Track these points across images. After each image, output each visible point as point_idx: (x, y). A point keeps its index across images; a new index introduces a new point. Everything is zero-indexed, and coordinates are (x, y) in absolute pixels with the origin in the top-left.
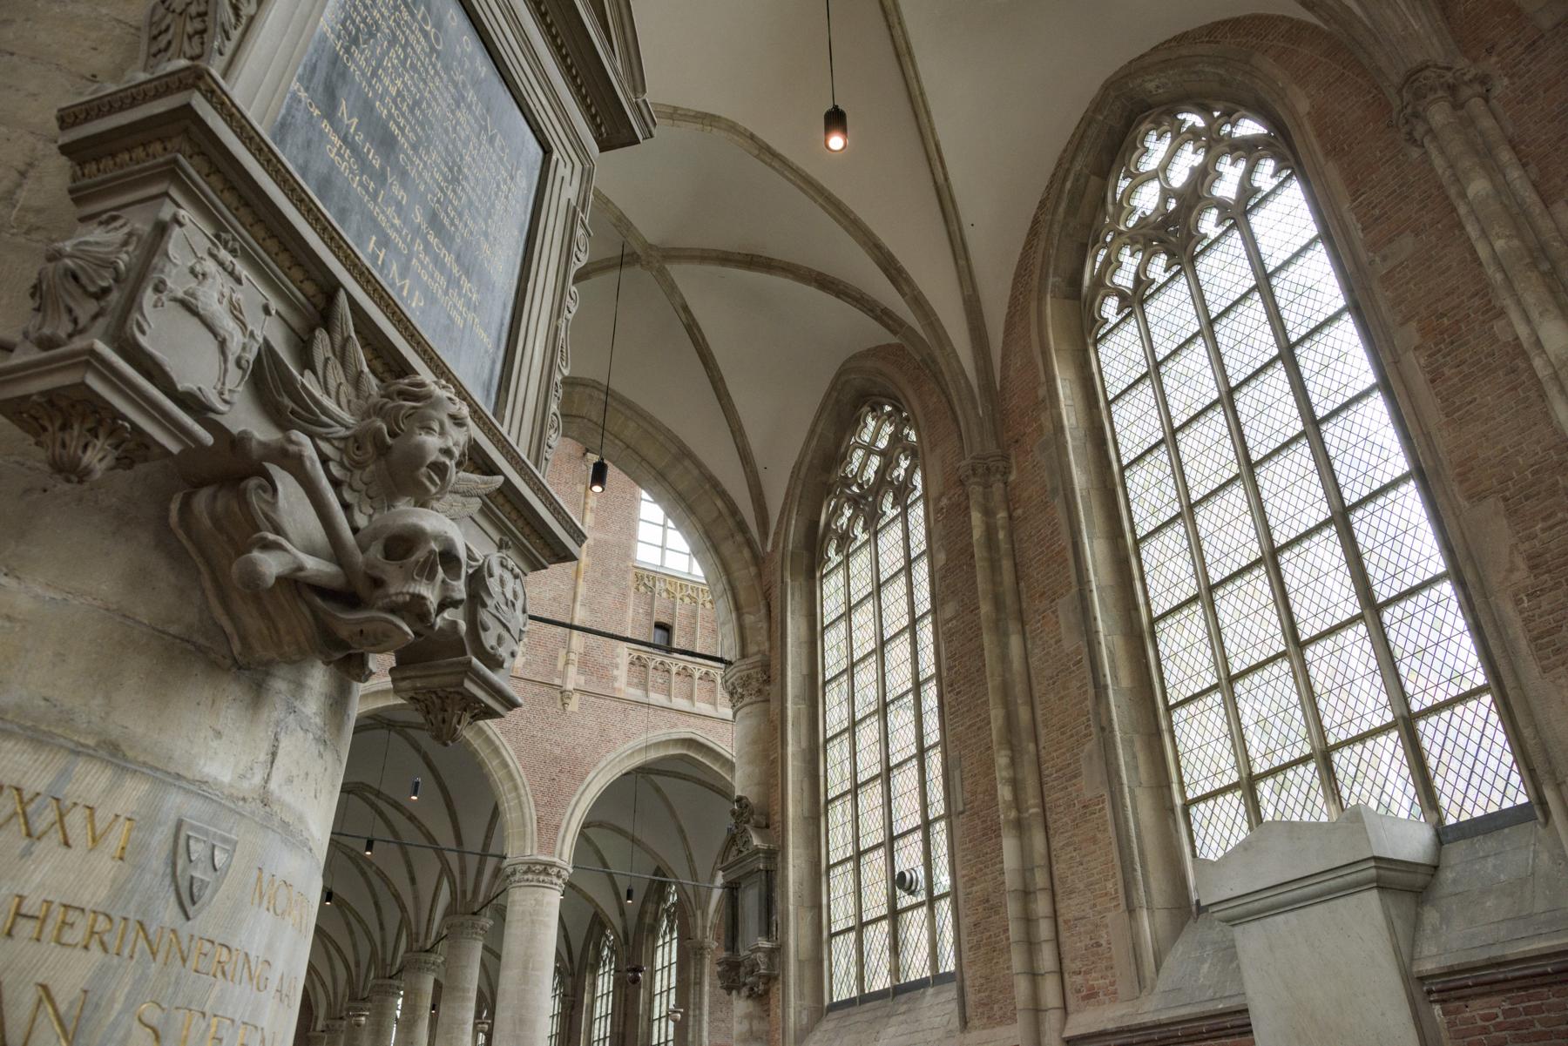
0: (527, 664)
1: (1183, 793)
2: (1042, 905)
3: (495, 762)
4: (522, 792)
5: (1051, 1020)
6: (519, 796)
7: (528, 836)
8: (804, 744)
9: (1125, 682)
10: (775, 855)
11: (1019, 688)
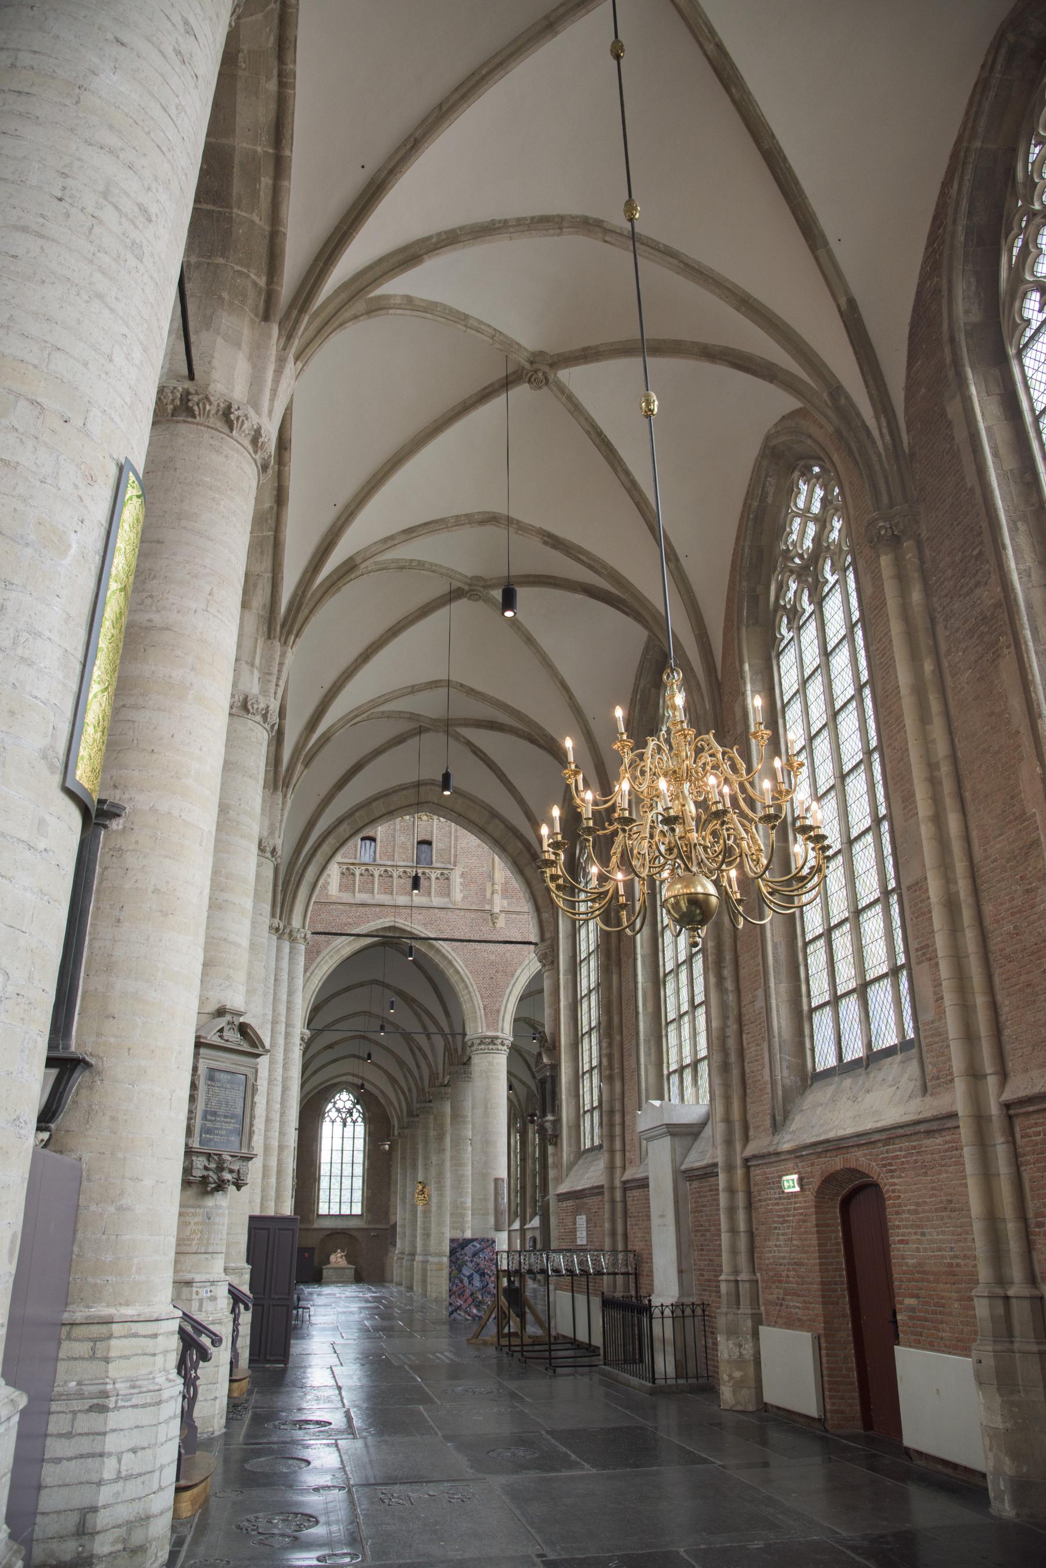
0: (465, 898)
1: (668, 1067)
2: (617, 1118)
3: (451, 971)
4: (471, 989)
5: (618, 1171)
6: (469, 992)
7: (479, 1020)
8: (570, 1000)
9: (650, 1009)
10: (555, 1067)
11: (615, 1004)
